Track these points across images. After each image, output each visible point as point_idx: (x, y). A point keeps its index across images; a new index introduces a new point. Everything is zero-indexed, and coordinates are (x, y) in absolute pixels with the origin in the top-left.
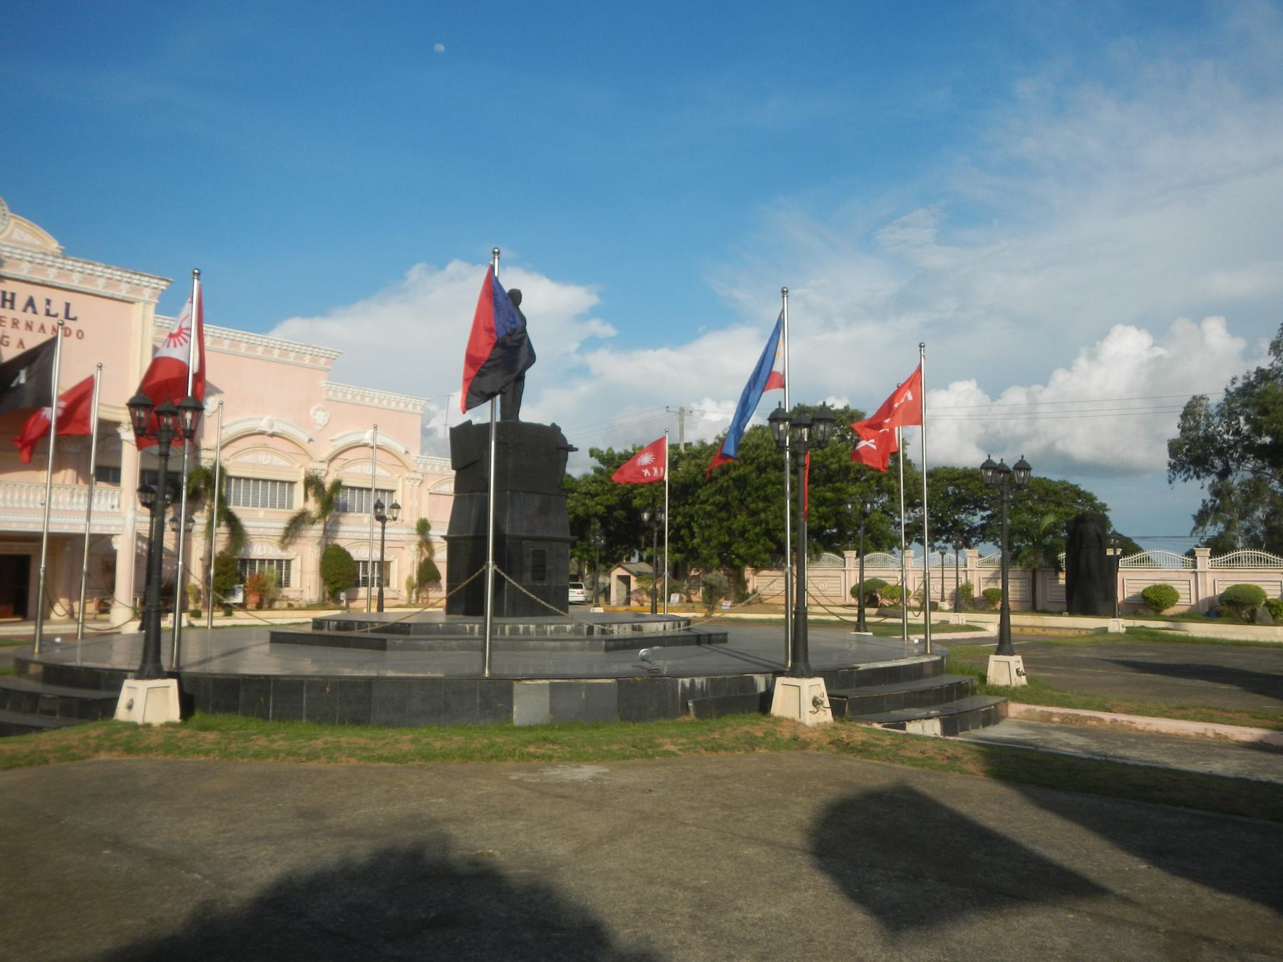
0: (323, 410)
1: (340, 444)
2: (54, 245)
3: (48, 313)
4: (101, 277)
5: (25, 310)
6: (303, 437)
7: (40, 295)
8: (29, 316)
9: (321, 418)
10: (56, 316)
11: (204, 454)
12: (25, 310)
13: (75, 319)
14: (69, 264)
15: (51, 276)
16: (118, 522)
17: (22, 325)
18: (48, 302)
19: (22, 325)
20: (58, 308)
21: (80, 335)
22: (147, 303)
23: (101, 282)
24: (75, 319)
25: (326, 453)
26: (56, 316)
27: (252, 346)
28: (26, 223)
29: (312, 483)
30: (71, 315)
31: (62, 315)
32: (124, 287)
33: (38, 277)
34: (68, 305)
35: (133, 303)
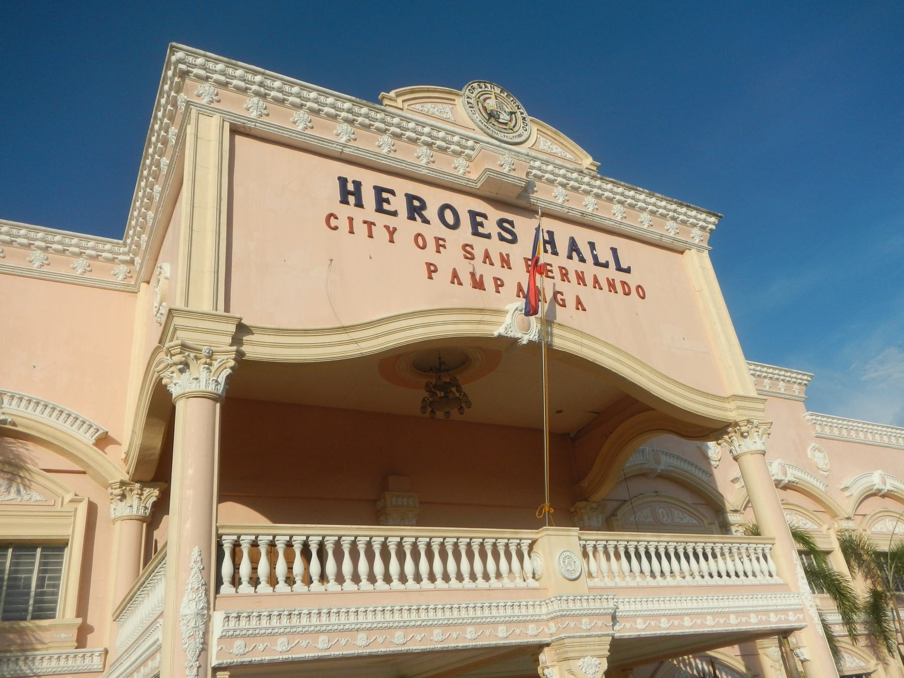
0: (820, 451)
1: (857, 491)
2: (587, 161)
3: (597, 263)
5: (570, 257)
6: (815, 484)
7: (583, 236)
8: (574, 265)
9: (820, 459)
10: (606, 265)
11: (732, 518)
12: (570, 257)
13: (628, 271)
15: (589, 205)
16: (792, 601)
17: (572, 276)
18: (592, 245)
19: (572, 276)
21: (641, 293)
23: (645, 216)
24: (628, 271)
25: (846, 505)
26: (606, 265)
28: (549, 129)
29: (852, 549)
31: (612, 264)
34: (614, 251)
35: (682, 252)
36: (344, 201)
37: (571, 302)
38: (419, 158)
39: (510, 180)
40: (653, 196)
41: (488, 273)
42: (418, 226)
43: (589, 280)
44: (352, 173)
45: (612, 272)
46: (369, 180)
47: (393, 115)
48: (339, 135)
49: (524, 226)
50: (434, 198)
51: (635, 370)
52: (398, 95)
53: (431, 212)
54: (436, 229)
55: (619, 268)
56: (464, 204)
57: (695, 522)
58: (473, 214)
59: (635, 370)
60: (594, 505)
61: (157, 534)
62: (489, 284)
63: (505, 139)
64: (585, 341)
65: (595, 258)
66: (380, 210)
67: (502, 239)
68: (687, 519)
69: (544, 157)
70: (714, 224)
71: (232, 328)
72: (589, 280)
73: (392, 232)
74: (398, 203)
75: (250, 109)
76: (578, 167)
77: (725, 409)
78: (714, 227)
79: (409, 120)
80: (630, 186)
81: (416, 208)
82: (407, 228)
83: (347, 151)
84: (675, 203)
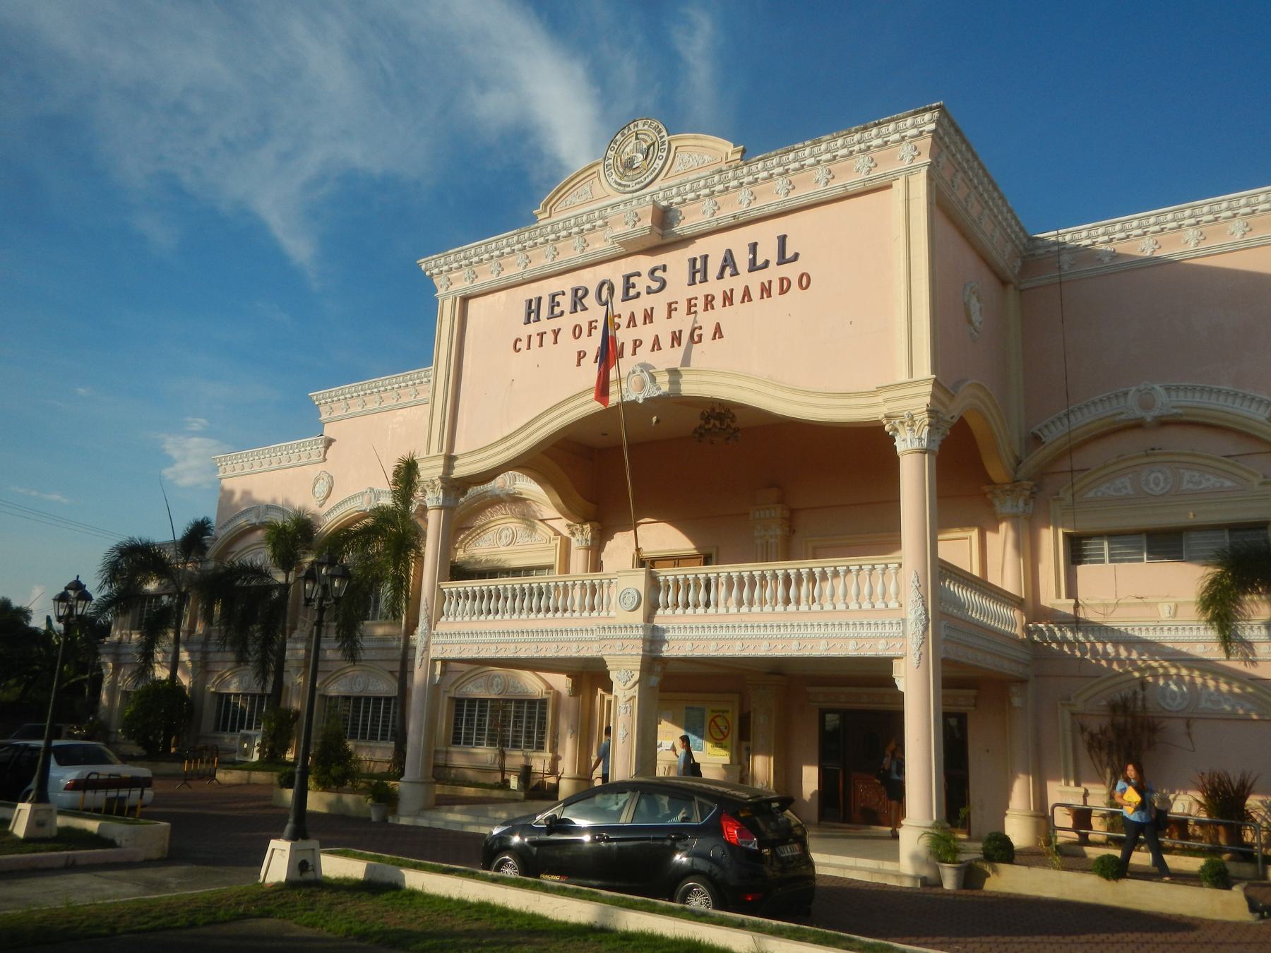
3: (753, 267)
5: (721, 276)
7: (737, 241)
8: (728, 282)
10: (766, 264)
12: (721, 276)
18: (754, 247)
19: (718, 302)
20: (768, 251)
21: (805, 281)
22: (910, 171)
24: (796, 257)
26: (766, 264)
30: (789, 255)
31: (774, 258)
32: (861, 161)
33: (727, 213)
34: (782, 240)
35: (890, 187)
36: (528, 321)
37: (708, 332)
38: (570, 253)
39: (636, 235)
40: (820, 142)
43: (738, 296)
44: (532, 291)
45: (774, 273)
46: (544, 289)
47: (545, 226)
48: (514, 270)
49: (676, 262)
50: (589, 279)
51: (759, 392)
52: (546, 205)
55: (782, 260)
56: (614, 273)
57: (1228, 483)
58: (627, 278)
59: (759, 392)
60: (1008, 487)
61: (603, 556)
63: (638, 186)
64: (705, 378)
65: (753, 261)
66: (552, 315)
67: (650, 291)
68: (1211, 481)
69: (677, 181)
70: (931, 121)
71: (442, 462)
72: (738, 296)
73: (556, 333)
74: (565, 302)
75: (462, 284)
76: (716, 167)
77: (878, 405)
78: (933, 126)
79: (557, 223)
80: (783, 150)
82: (566, 323)
83: (525, 276)
84: (857, 131)
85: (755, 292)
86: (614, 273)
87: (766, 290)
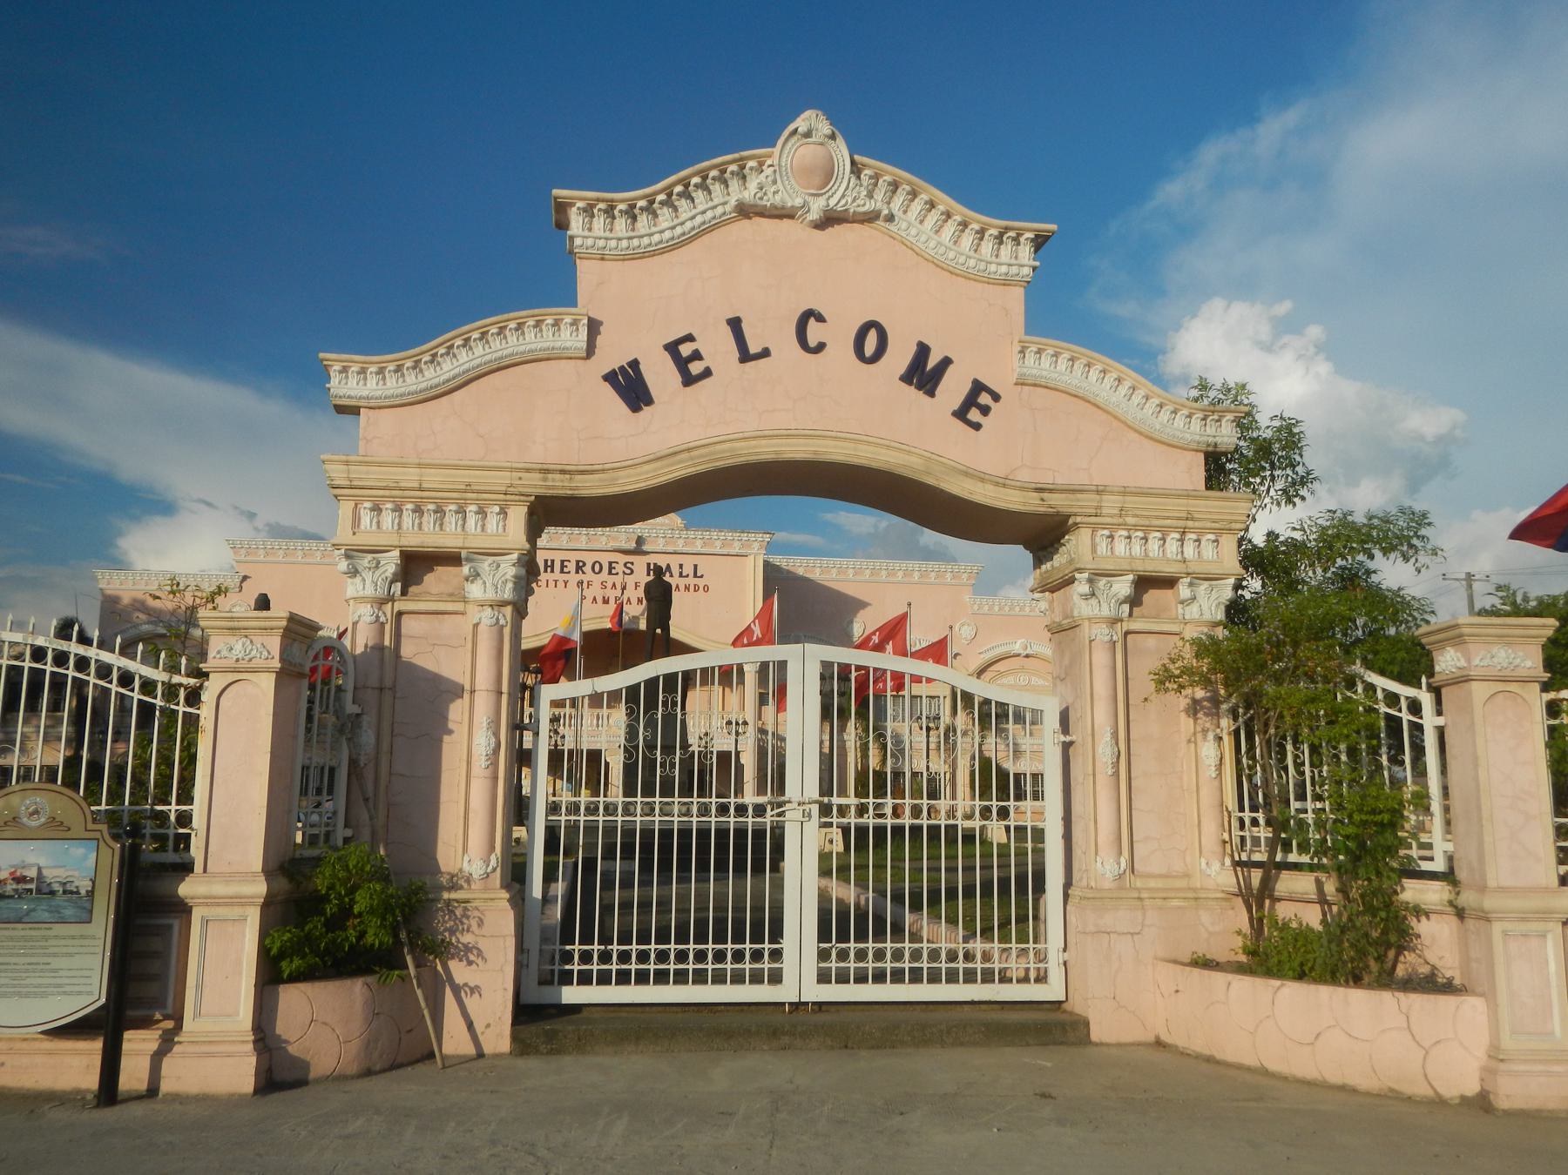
1: (988, 656)
4: (718, 539)
14: (691, 534)
18: (681, 566)
20: (688, 570)
21: (706, 589)
25: (975, 664)
27: (891, 573)
33: (670, 549)
41: (612, 594)
42: (580, 576)
45: (691, 581)
53: (588, 569)
54: (589, 575)
62: (612, 601)
74: (572, 567)
81: (579, 567)
82: (574, 578)
85: (682, 587)
86: (605, 559)
87: (687, 588)
